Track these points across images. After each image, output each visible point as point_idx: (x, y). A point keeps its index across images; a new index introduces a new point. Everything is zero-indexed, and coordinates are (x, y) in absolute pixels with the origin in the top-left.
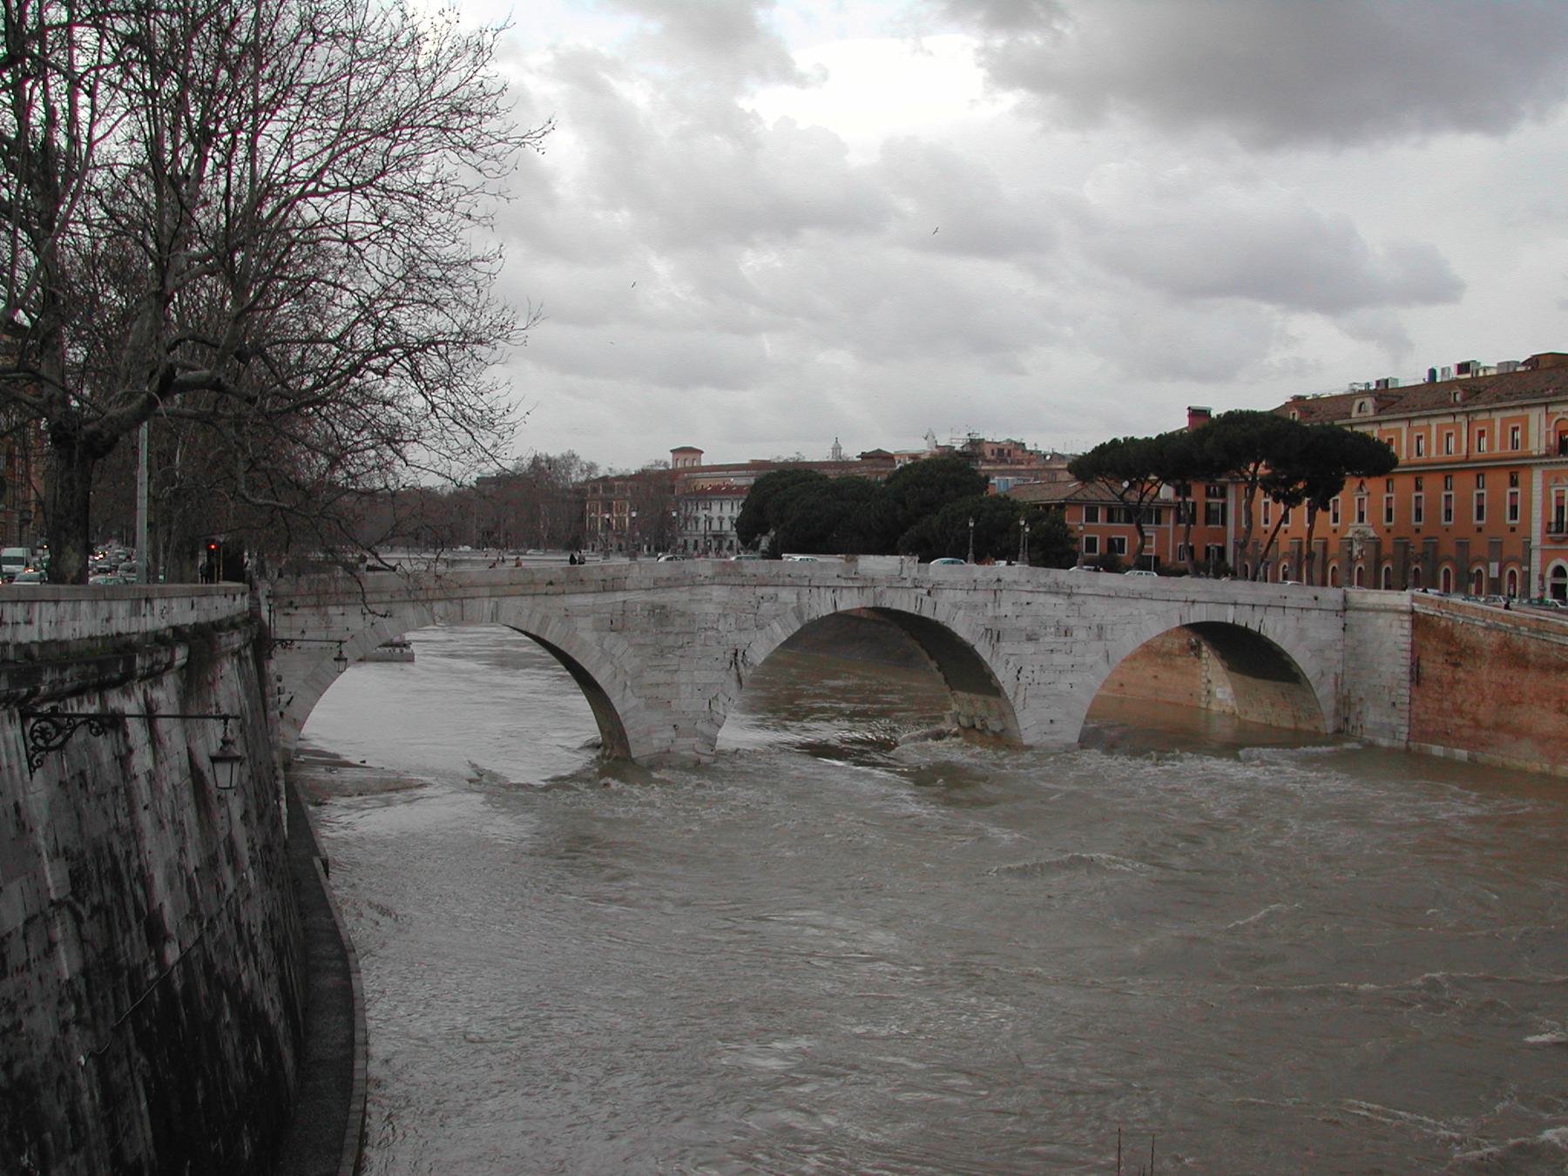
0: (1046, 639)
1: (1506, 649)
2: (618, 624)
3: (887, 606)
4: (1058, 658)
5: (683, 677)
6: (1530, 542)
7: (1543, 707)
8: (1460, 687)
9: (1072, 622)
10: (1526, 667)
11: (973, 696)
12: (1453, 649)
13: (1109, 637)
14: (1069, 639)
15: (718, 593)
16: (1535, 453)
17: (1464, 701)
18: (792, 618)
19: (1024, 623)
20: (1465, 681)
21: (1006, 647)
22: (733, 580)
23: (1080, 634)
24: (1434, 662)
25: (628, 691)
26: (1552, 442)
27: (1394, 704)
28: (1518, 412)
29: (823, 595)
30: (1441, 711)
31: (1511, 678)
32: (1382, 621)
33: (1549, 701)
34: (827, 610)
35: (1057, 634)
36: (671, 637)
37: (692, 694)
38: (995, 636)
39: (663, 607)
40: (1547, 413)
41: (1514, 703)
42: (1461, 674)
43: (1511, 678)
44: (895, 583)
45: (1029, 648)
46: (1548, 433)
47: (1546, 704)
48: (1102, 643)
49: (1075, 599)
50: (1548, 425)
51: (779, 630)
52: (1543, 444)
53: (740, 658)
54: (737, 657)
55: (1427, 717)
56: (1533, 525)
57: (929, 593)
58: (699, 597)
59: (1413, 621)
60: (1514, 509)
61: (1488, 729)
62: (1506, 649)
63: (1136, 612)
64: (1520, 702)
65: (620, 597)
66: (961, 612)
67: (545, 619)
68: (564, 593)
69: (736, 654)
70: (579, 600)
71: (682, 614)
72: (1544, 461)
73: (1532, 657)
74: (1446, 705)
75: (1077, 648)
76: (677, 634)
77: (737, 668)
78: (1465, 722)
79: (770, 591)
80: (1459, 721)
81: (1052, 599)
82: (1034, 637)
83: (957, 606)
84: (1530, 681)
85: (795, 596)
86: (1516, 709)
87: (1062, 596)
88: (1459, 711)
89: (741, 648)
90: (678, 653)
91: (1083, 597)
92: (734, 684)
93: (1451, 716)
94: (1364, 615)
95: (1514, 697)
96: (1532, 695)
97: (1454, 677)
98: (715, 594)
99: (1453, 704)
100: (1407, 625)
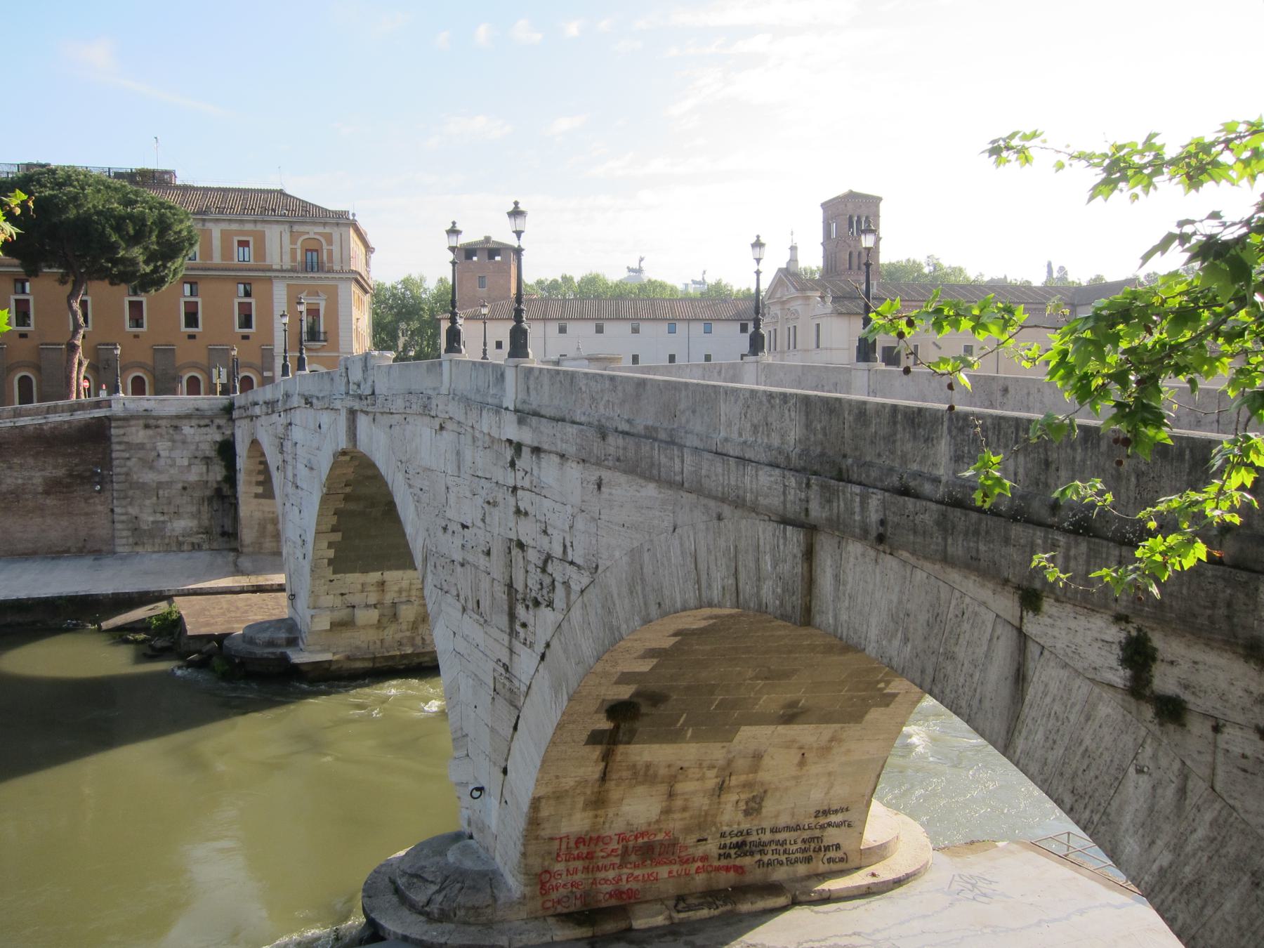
6: (272, 350)
16: (278, 267)
26: (299, 258)
28: (249, 227)
40: (291, 232)
46: (293, 252)
50: (293, 242)
52: (287, 258)
56: (276, 334)
60: (246, 322)
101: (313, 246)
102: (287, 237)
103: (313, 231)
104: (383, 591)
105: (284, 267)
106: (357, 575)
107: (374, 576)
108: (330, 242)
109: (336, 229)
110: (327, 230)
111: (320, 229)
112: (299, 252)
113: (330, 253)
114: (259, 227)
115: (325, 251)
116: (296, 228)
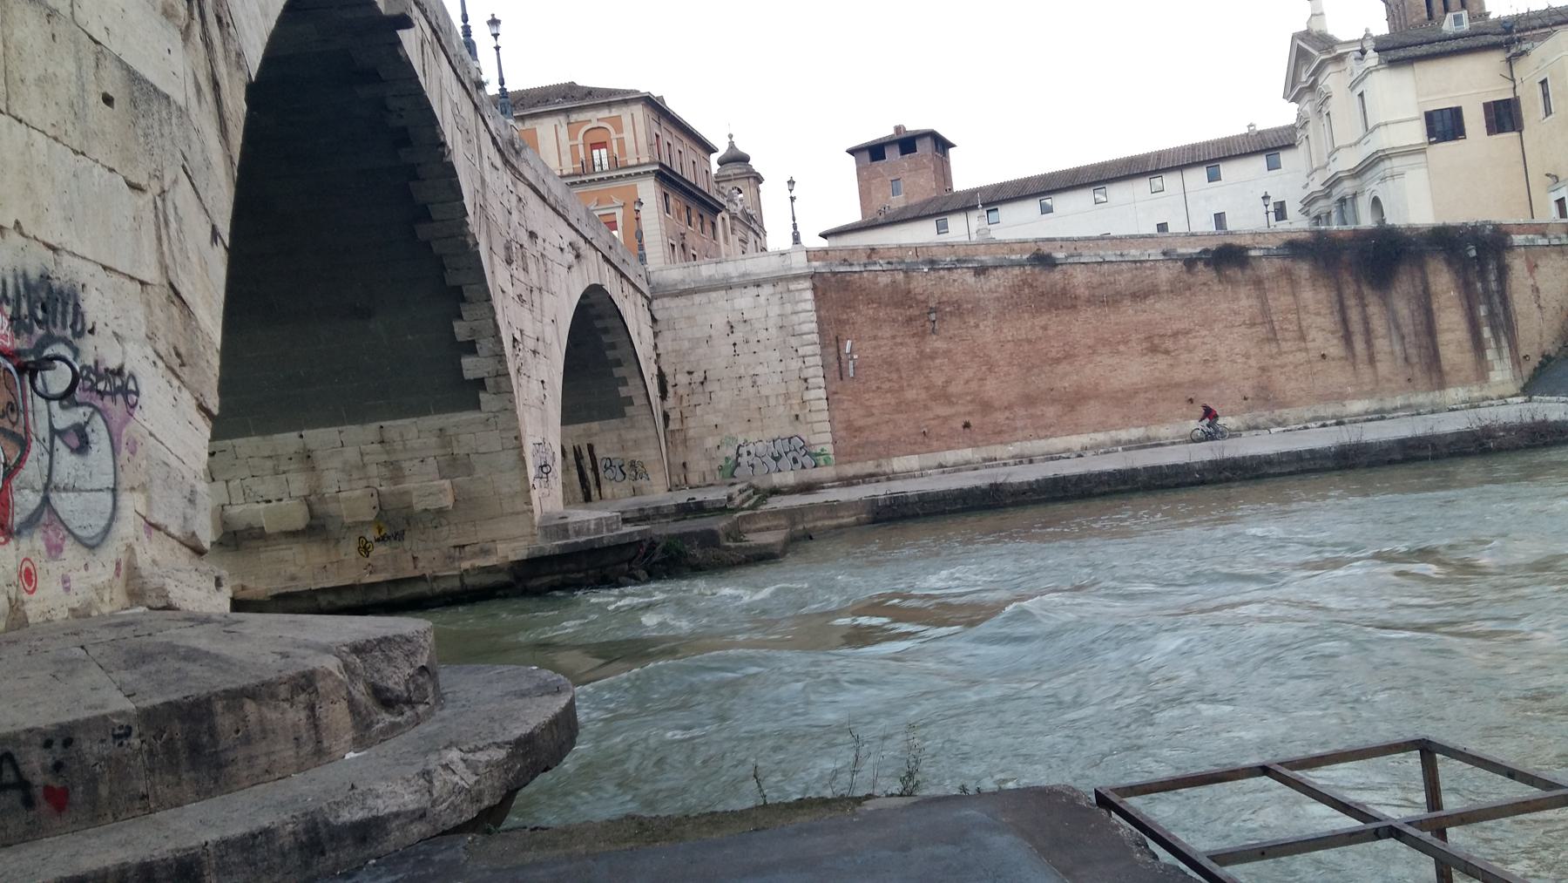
1: (1027, 291)
7: (1118, 352)
8: (938, 361)
10: (1074, 307)
11: (318, 437)
12: (915, 312)
17: (948, 382)
20: (947, 353)
24: (875, 338)
26: (582, 155)
27: (797, 416)
30: (902, 406)
31: (1045, 328)
32: (744, 301)
33: (1126, 342)
41: (1058, 361)
42: (938, 344)
43: (1045, 328)
46: (574, 149)
47: (1122, 348)
50: (572, 135)
52: (567, 159)
55: (871, 421)
59: (814, 288)
61: (1009, 407)
62: (1027, 291)
64: (1068, 357)
72: (578, 179)
73: (1082, 292)
74: (910, 394)
78: (962, 409)
80: (942, 410)
84: (1081, 325)
86: (1064, 367)
88: (945, 397)
93: (926, 407)
94: (697, 298)
95: (1053, 354)
96: (1090, 342)
97: (921, 353)
99: (927, 389)
100: (809, 295)
101: (597, 137)
102: (564, 131)
103: (594, 117)
104: (313, 469)
105: (565, 172)
106: (255, 440)
107: (288, 441)
108: (619, 129)
109: (625, 109)
110: (615, 112)
111: (604, 113)
112: (581, 148)
113: (621, 142)
114: (529, 124)
115: (615, 143)
116: (574, 117)
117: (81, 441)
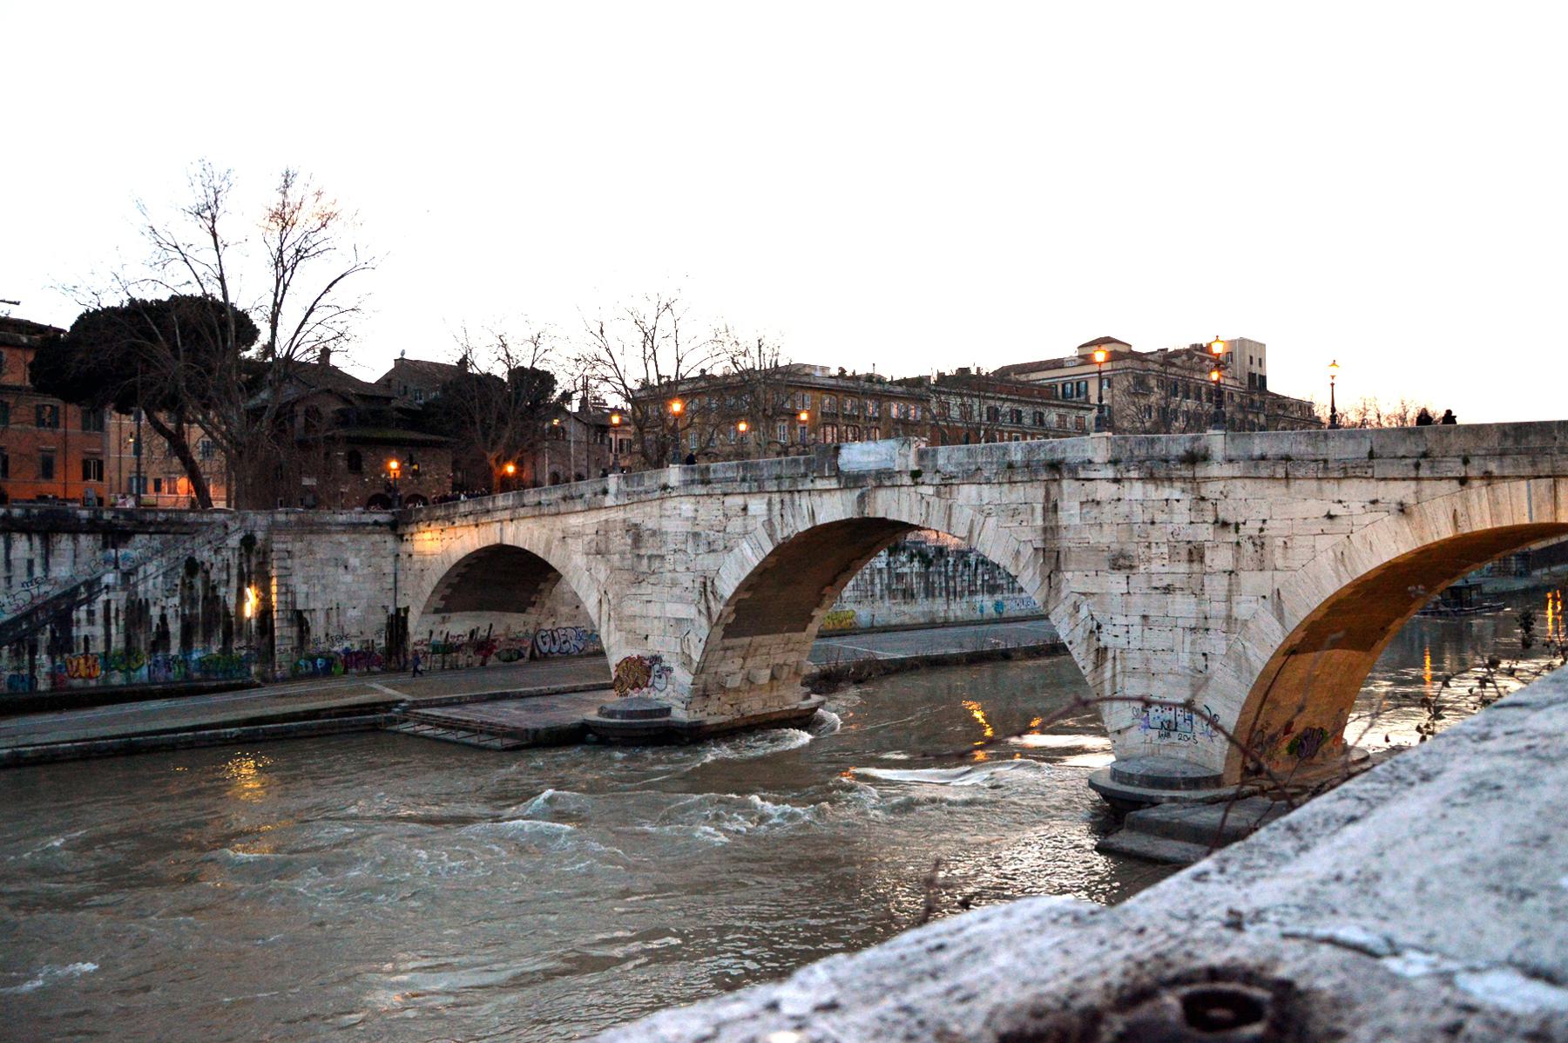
0: (1155, 566)
2: (603, 547)
3: (880, 514)
4: (1183, 606)
5: (654, 610)
9: (1205, 533)
13: (1280, 563)
14: (1196, 567)
15: (687, 507)
18: (762, 534)
19: (1107, 537)
21: (1073, 580)
22: (699, 490)
23: (1220, 558)
25: (612, 623)
29: (797, 503)
34: (804, 525)
35: (1173, 555)
36: (645, 561)
37: (664, 630)
38: (1052, 559)
39: (636, 525)
44: (884, 477)
45: (1115, 583)
48: (1268, 574)
49: (1210, 490)
51: (749, 552)
53: (709, 589)
54: (707, 588)
57: (938, 494)
58: (668, 513)
63: (1336, 509)
65: (603, 515)
66: (992, 521)
67: (548, 544)
68: (558, 514)
69: (705, 584)
70: (574, 521)
71: (654, 533)
75: (1217, 586)
76: (650, 557)
77: (707, 601)
79: (739, 501)
81: (1166, 492)
82: (1121, 561)
83: (983, 511)
85: (765, 507)
87: (1178, 485)
89: (710, 574)
90: (652, 579)
91: (1222, 483)
92: (704, 621)
98: (684, 507)
117: (660, 677)
